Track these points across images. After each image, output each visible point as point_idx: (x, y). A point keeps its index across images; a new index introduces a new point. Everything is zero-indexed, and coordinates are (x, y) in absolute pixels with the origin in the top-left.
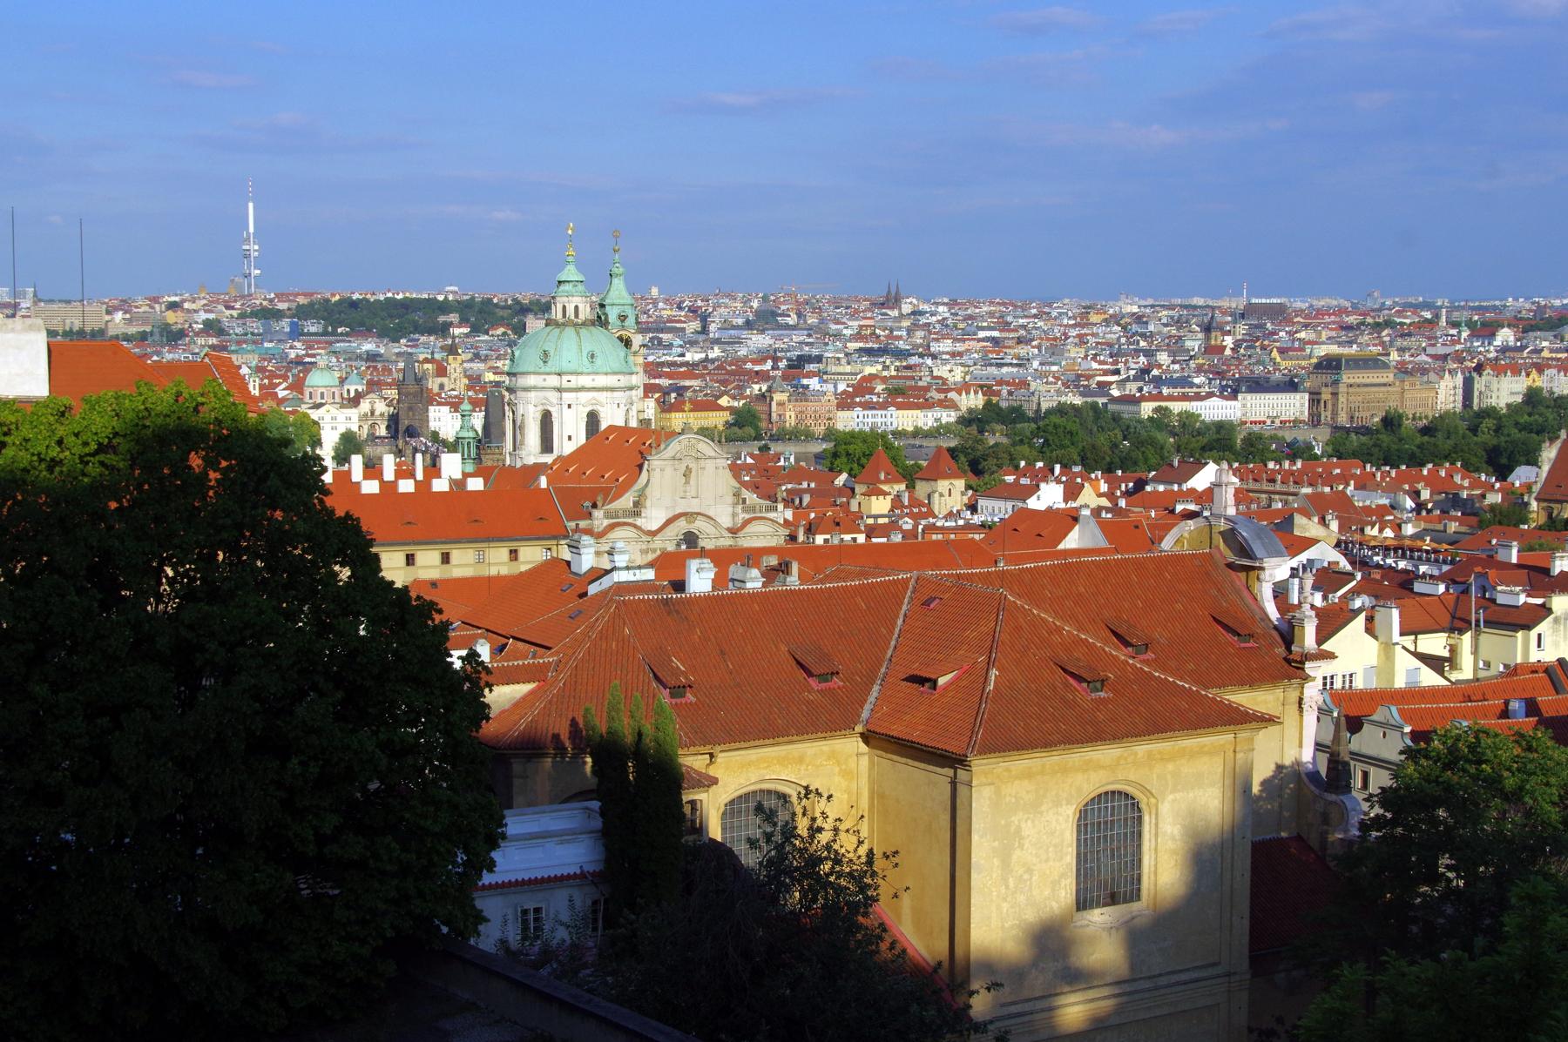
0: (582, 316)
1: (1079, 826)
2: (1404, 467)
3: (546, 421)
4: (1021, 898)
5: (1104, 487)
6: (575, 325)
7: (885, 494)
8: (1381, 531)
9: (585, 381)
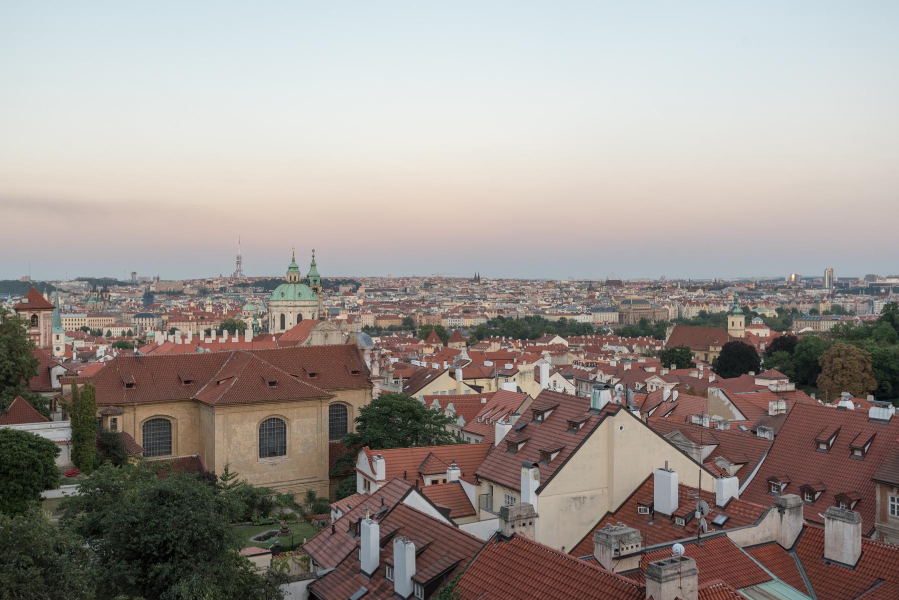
0: (297, 280)
1: (260, 430)
2: (630, 337)
3: (283, 318)
4: (236, 453)
5: (520, 345)
6: (294, 283)
7: (432, 347)
9: (280, 303)
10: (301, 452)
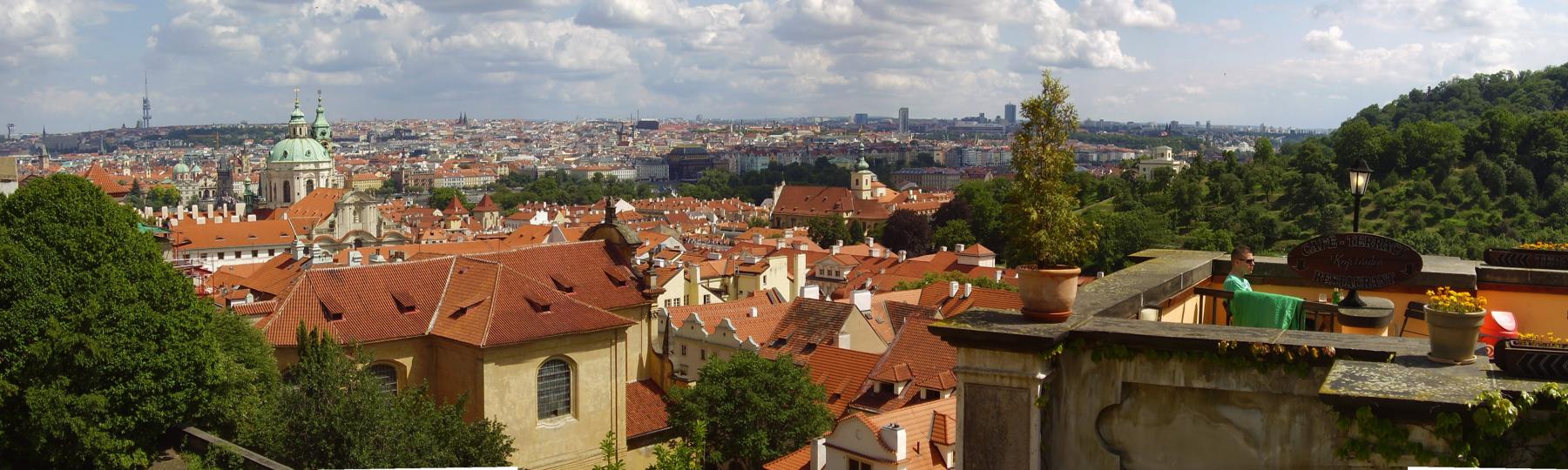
0: (303, 134)
5: (568, 213)
6: (300, 138)
7: (458, 220)
8: (702, 231)
10: (591, 409)
